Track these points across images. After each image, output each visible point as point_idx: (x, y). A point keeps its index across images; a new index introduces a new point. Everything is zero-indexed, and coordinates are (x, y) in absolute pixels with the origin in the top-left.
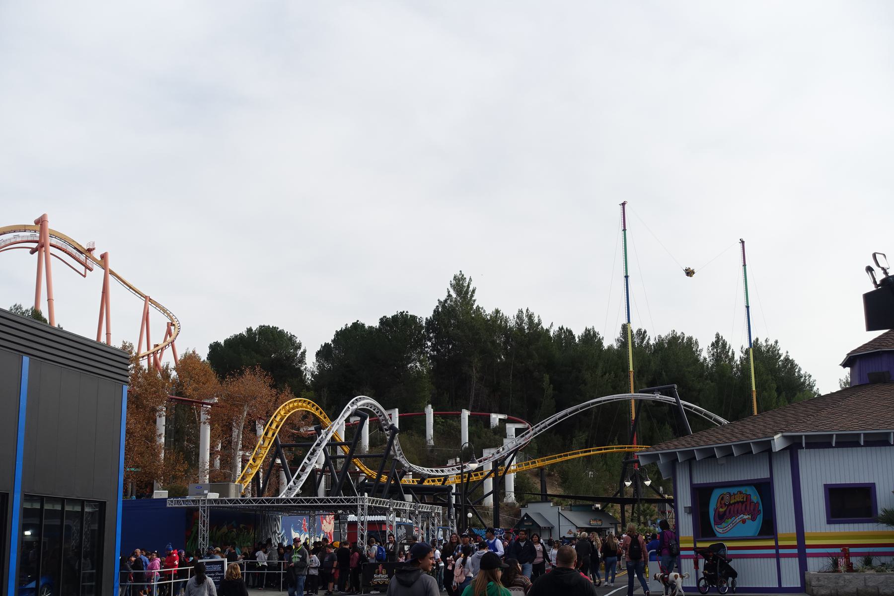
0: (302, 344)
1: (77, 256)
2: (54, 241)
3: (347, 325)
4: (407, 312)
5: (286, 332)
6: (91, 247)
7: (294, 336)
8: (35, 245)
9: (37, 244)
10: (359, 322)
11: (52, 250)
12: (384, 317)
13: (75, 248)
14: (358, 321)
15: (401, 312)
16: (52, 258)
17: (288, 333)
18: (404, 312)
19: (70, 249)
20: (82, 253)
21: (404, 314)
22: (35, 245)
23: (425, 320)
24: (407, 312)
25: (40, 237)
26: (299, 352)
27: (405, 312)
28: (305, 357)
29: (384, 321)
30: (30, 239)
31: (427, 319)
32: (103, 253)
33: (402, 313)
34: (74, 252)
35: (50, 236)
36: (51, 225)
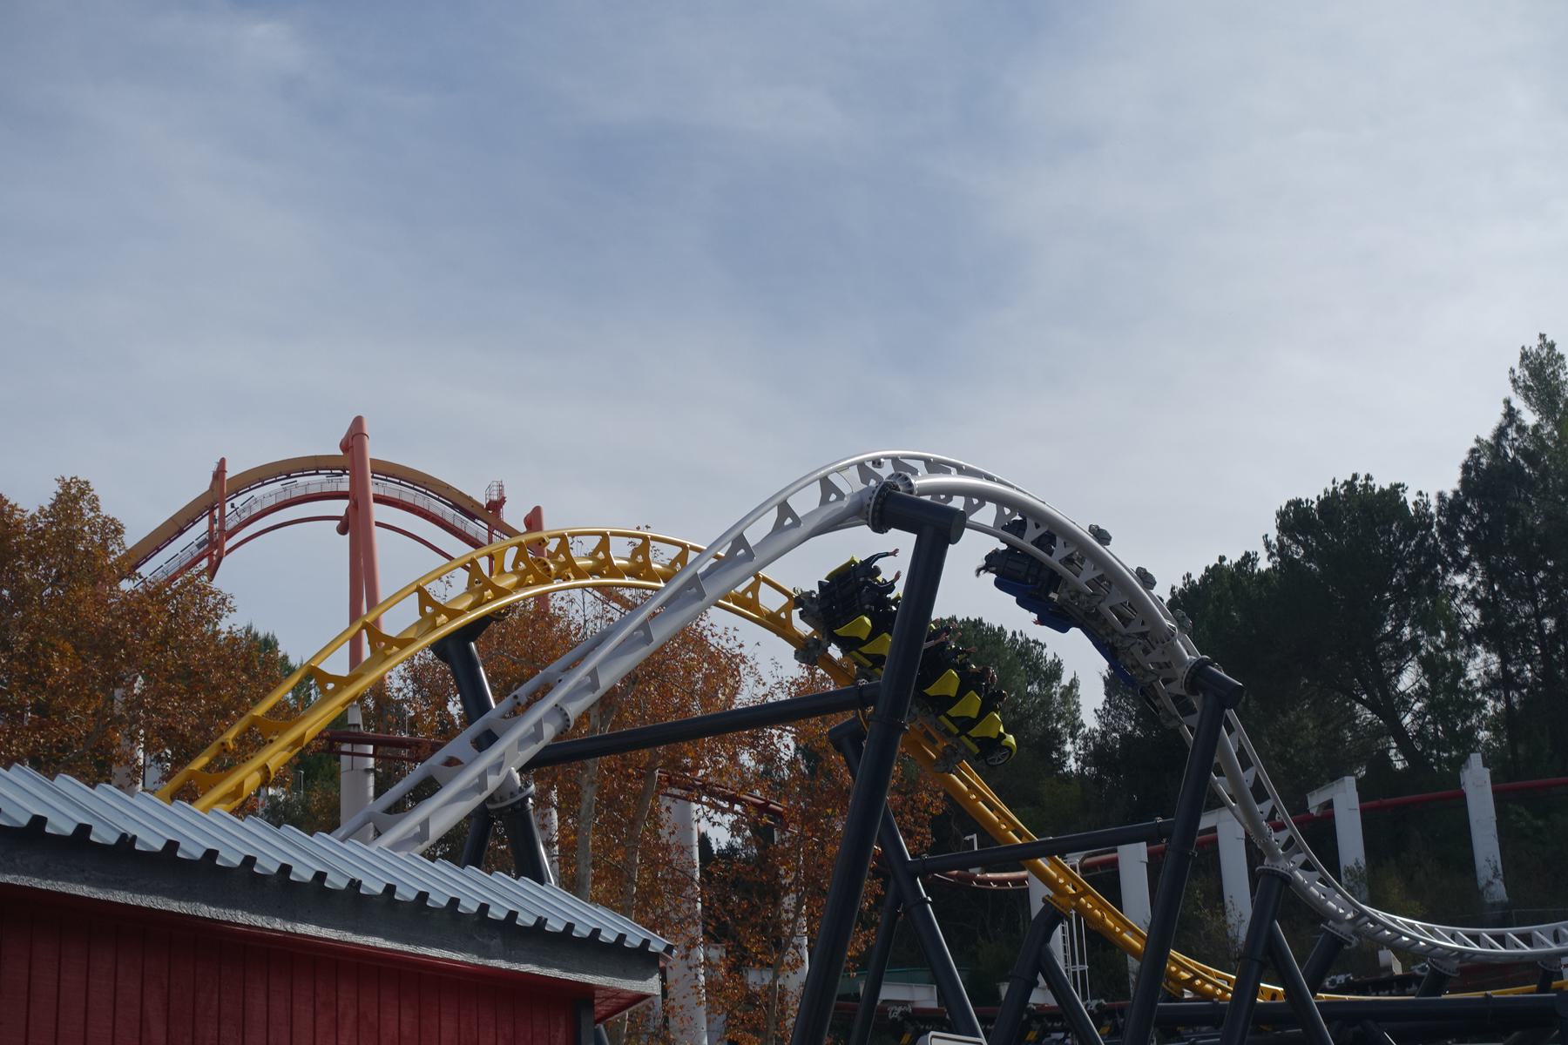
0: (1065, 665)
1: (458, 524)
2: (392, 489)
3: (1189, 575)
4: (1368, 477)
5: (1009, 635)
6: (495, 498)
7: (1036, 642)
8: (340, 507)
9: (345, 503)
10: (1226, 563)
11: (379, 512)
12: (1289, 504)
13: (455, 506)
14: (1222, 559)
15: (1346, 483)
16: (378, 532)
17: (1018, 637)
18: (1355, 477)
19: (438, 507)
20: (472, 517)
21: (1358, 482)
22: (340, 507)
23: (1434, 503)
24: (1368, 477)
25: (352, 482)
26: (1057, 690)
27: (1362, 477)
28: (1078, 705)
29: (1295, 519)
30: (328, 488)
31: (1441, 496)
32: (529, 511)
33: (1350, 485)
34: (450, 514)
35: (373, 477)
36: (375, 450)
